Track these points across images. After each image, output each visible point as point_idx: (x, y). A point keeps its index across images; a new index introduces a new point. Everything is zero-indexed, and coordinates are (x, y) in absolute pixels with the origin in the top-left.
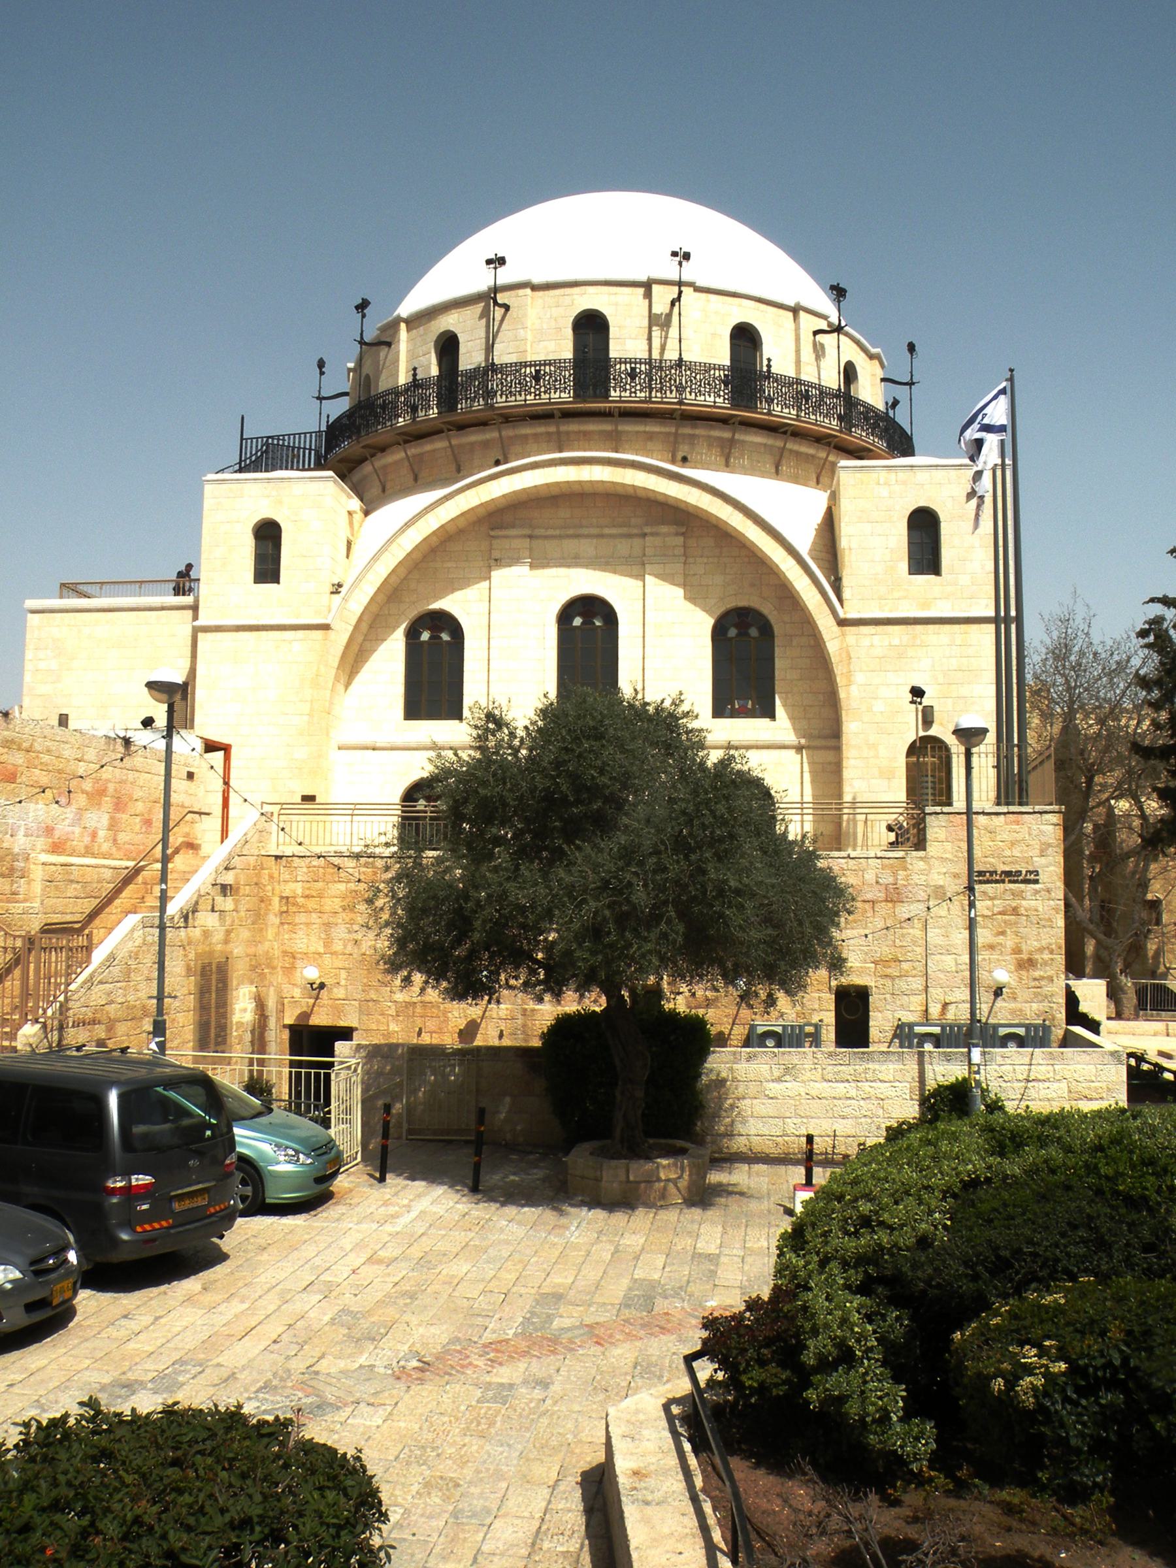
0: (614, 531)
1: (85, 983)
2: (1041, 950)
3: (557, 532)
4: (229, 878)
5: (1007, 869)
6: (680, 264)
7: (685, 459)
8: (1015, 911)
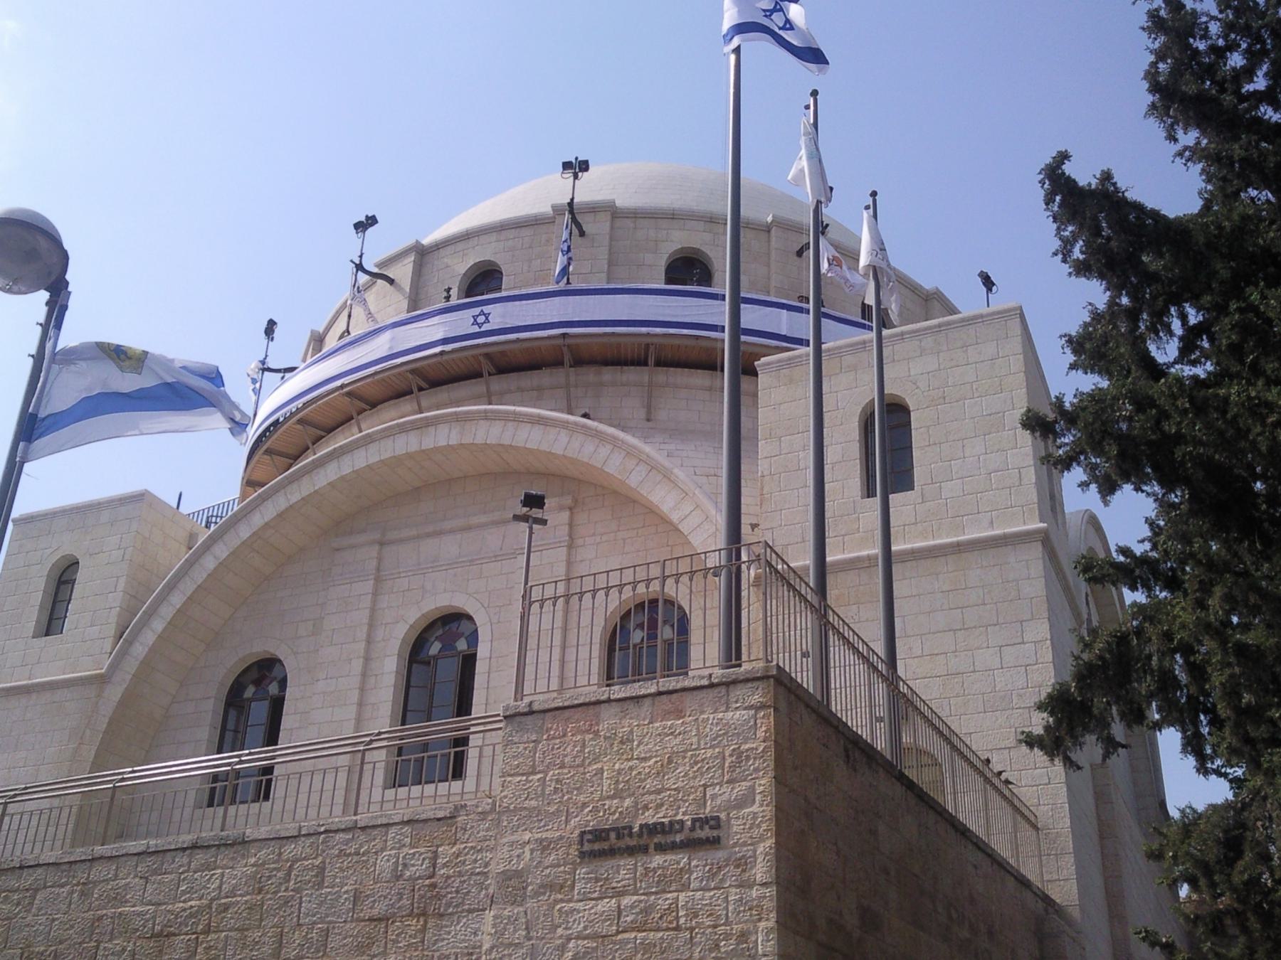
0: (483, 519)
3: (414, 532)
6: (576, 177)
7: (585, 416)
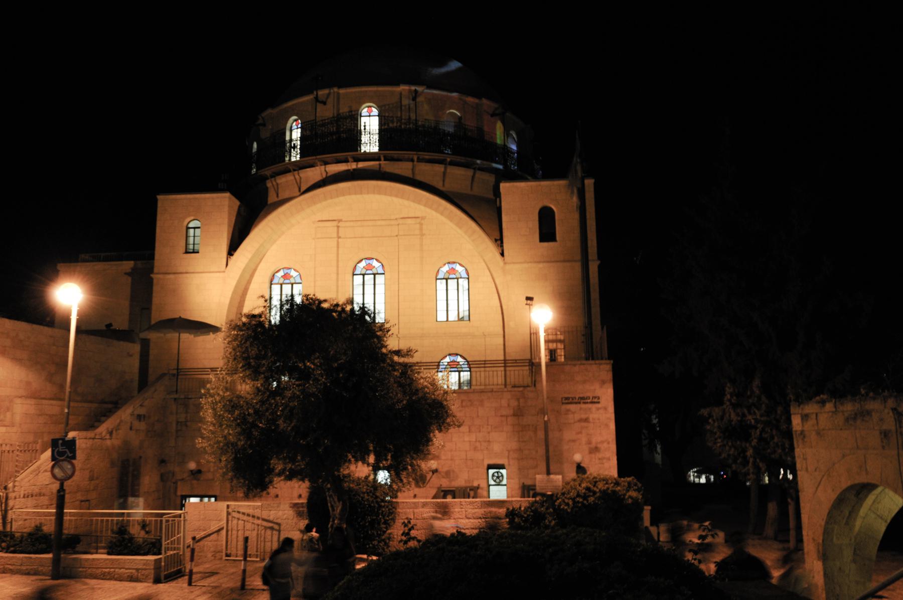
1: (34, 471)
2: (602, 442)
4: (142, 411)
5: (581, 396)
8: (586, 420)
